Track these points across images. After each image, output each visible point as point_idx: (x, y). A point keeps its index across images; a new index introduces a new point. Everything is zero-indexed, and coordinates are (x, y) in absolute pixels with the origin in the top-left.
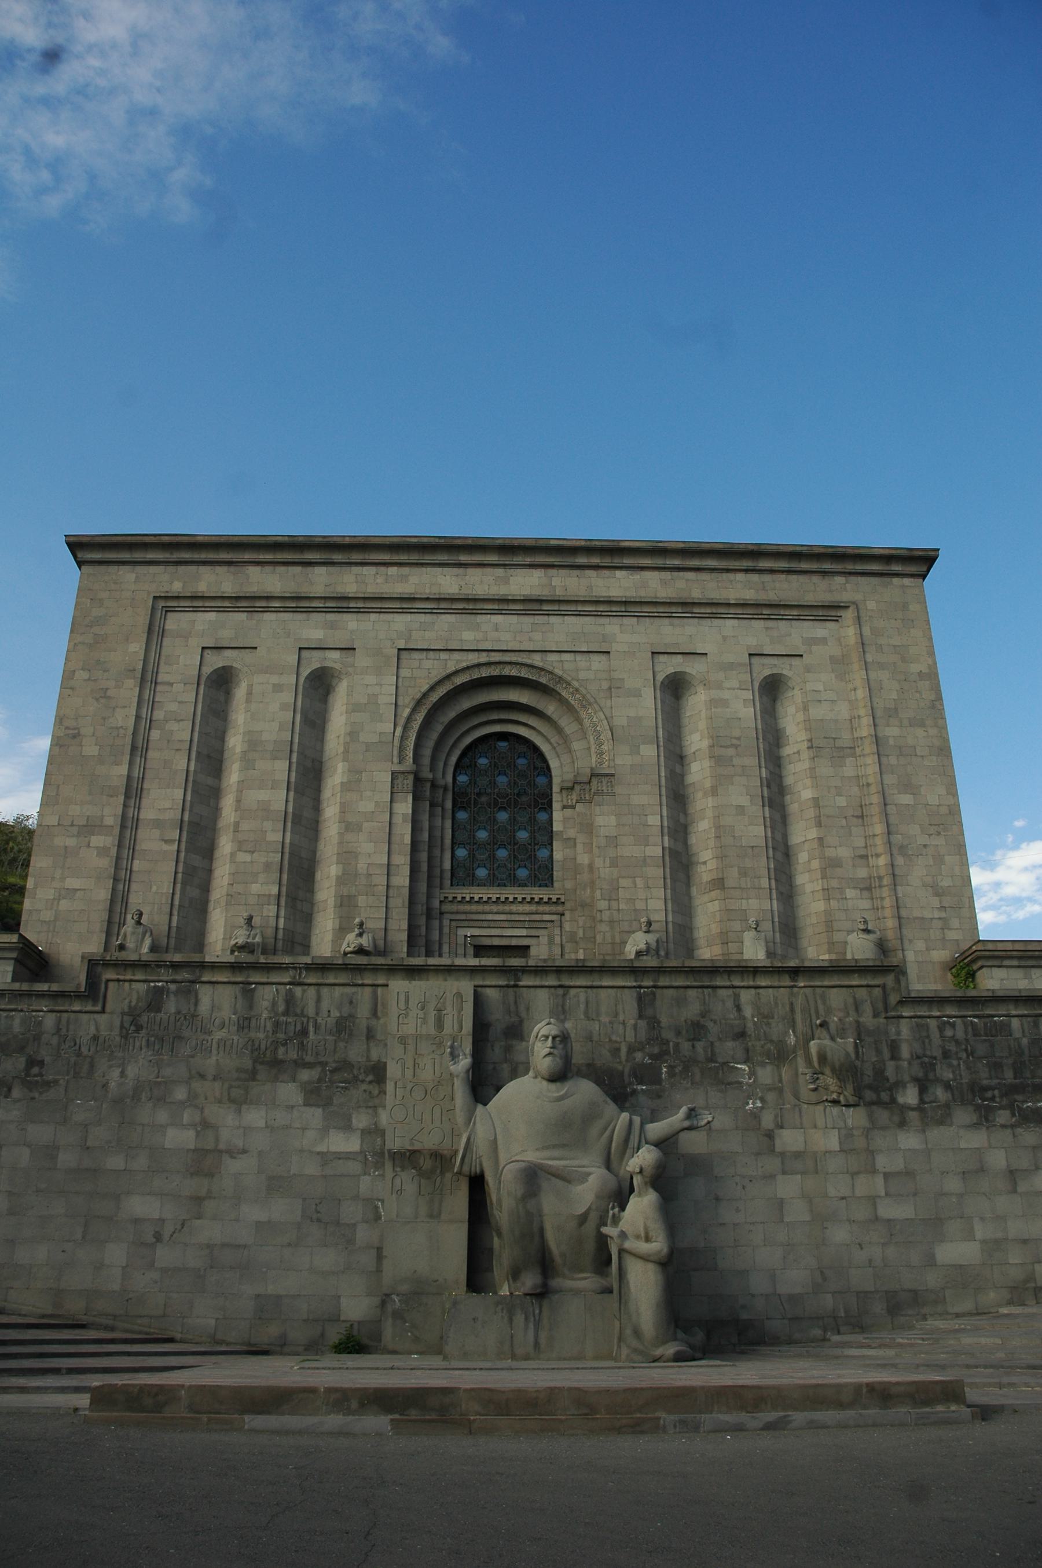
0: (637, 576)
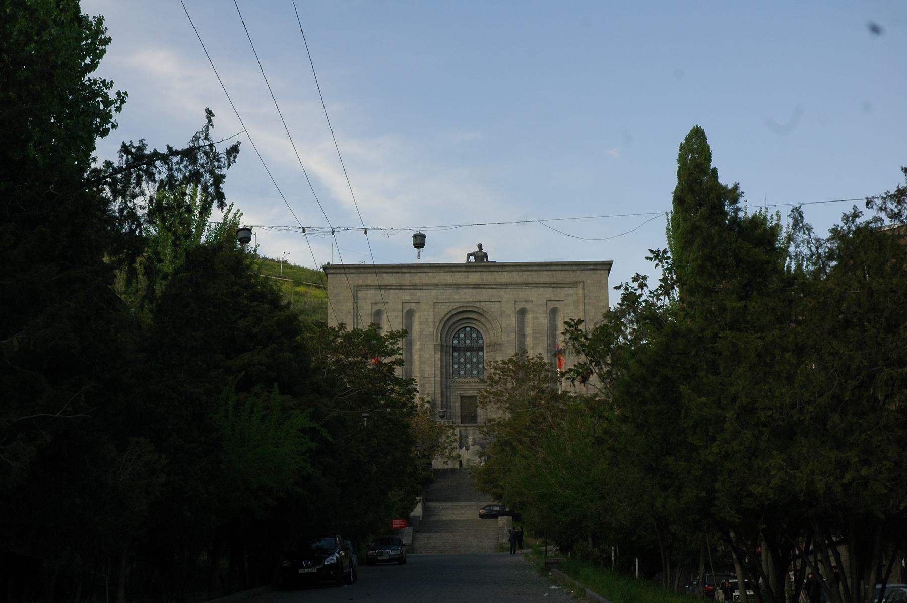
0: (511, 274)
